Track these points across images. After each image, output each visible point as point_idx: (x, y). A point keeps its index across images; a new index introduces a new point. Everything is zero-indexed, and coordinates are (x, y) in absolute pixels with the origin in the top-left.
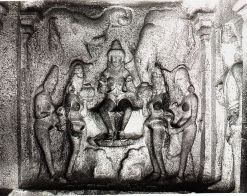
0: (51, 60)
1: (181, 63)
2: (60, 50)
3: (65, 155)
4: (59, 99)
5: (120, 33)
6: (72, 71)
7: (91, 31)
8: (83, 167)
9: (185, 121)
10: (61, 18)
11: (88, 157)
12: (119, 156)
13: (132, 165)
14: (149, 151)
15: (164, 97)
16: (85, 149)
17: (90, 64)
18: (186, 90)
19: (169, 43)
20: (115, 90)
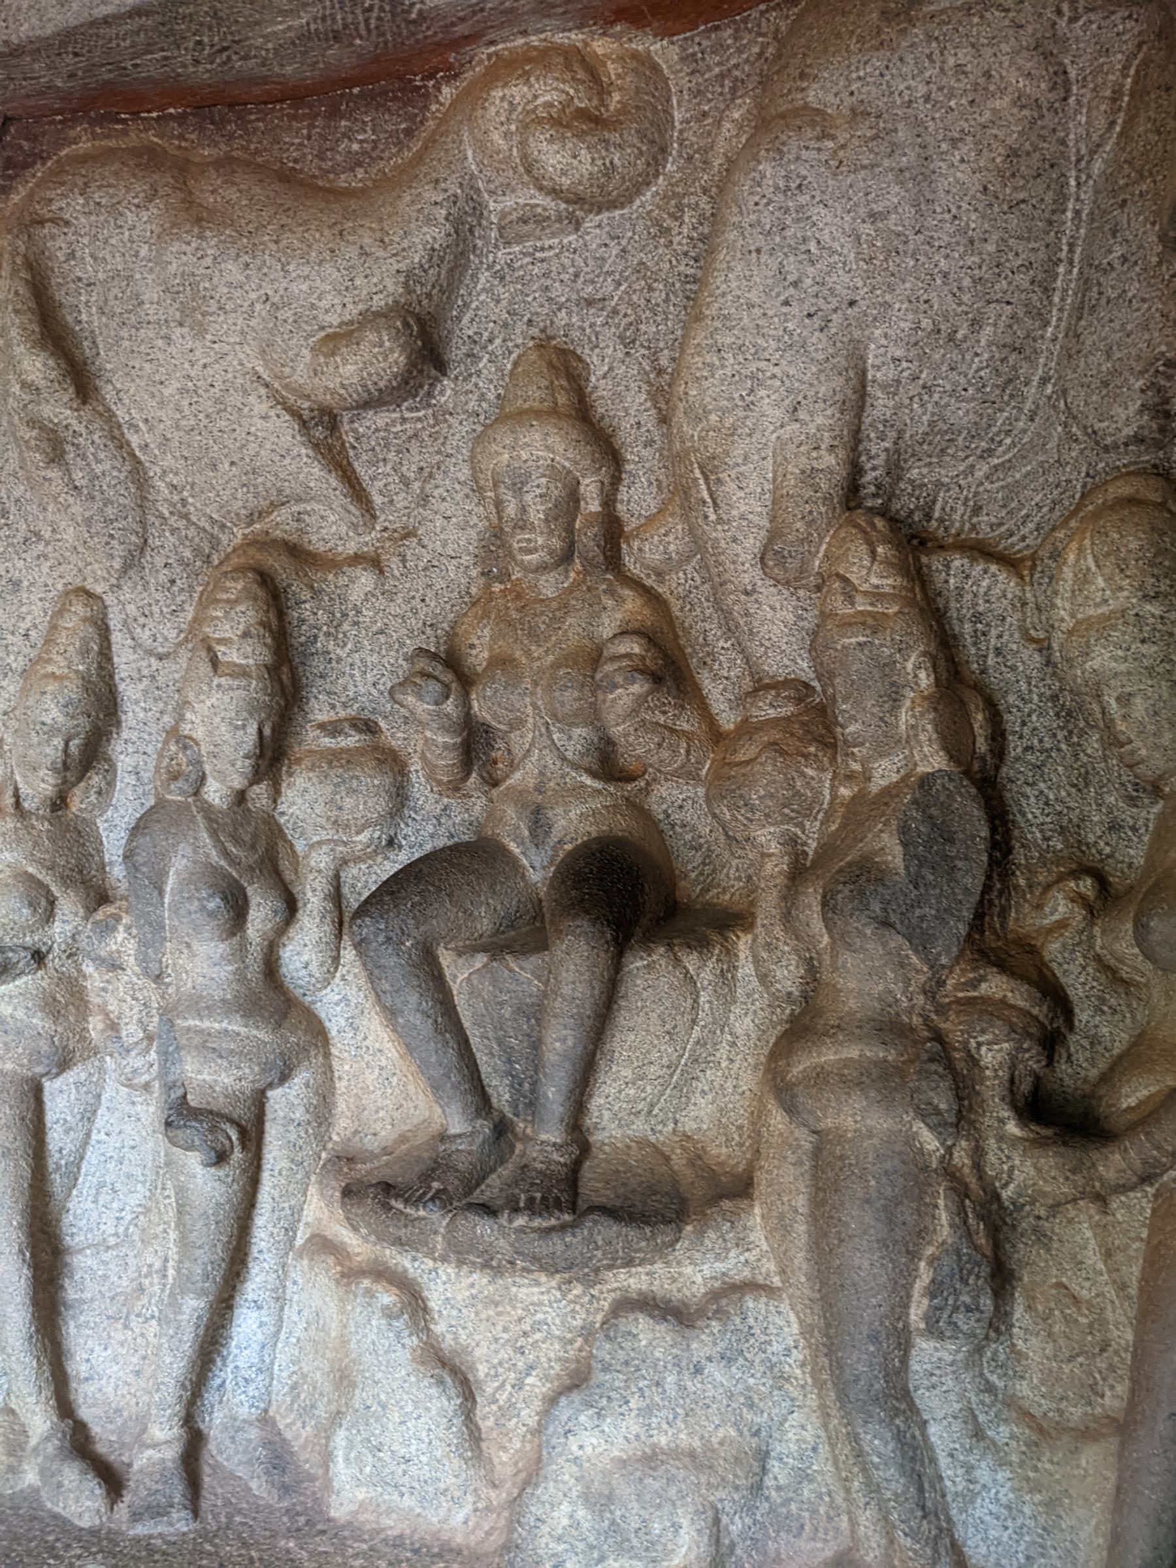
0: (50, 548)
5: (577, 275)
7: (304, 287)
8: (294, 1387)
10: (93, 218)
15: (934, 811)
17: (357, 559)
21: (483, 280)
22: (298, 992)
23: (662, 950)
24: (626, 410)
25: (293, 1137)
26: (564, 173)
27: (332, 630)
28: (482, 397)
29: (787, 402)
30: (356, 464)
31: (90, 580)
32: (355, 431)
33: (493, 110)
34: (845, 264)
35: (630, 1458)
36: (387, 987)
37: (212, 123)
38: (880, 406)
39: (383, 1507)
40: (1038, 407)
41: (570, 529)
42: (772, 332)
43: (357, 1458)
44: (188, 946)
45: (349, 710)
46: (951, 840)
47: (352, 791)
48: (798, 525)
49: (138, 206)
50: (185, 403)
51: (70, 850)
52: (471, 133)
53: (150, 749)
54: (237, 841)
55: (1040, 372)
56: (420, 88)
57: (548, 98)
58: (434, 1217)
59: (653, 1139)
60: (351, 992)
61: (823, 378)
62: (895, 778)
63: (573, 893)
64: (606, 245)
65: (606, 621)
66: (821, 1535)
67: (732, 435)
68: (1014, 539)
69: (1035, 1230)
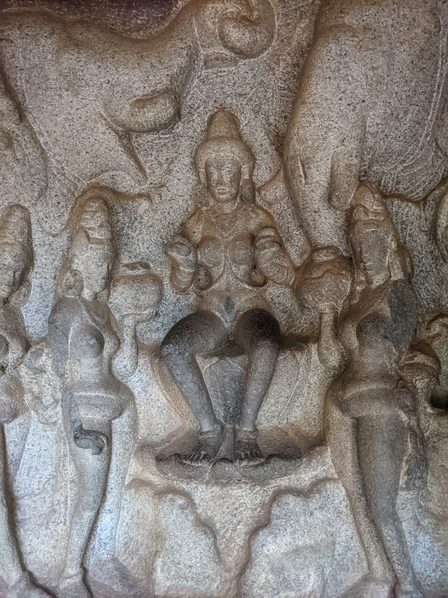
3: (62, 506)
7: (126, 78)
8: (125, 544)
10: (24, 40)
11: (138, 512)
12: (241, 513)
13: (286, 554)
14: (349, 495)
15: (398, 294)
16: (129, 487)
17: (140, 195)
19: (410, 93)
20: (223, 280)
21: (195, 82)
22: (120, 378)
23: (289, 352)
24: (256, 139)
25: (124, 439)
26: (238, 41)
27: (130, 225)
28: (195, 131)
29: (340, 138)
30: (138, 156)
31: (22, 201)
32: (138, 142)
33: (208, 12)
34: (362, 86)
35: (288, 552)
36: (179, 373)
38: (370, 141)
39: (179, 587)
40: (424, 145)
41: (238, 185)
42: (335, 110)
43: (167, 569)
44: (79, 360)
45: (137, 259)
46: (404, 305)
48: (345, 185)
49: (46, 37)
50: (67, 125)
51: (12, 321)
52: (197, 20)
53: (48, 276)
54: (98, 315)
55: (425, 132)
57: (232, 10)
58: (206, 466)
59: (279, 426)
61: (354, 129)
62: (382, 282)
63: (260, 331)
64: (247, 72)
66: (356, 570)
67: (317, 149)
68: (414, 194)
69: (434, 447)
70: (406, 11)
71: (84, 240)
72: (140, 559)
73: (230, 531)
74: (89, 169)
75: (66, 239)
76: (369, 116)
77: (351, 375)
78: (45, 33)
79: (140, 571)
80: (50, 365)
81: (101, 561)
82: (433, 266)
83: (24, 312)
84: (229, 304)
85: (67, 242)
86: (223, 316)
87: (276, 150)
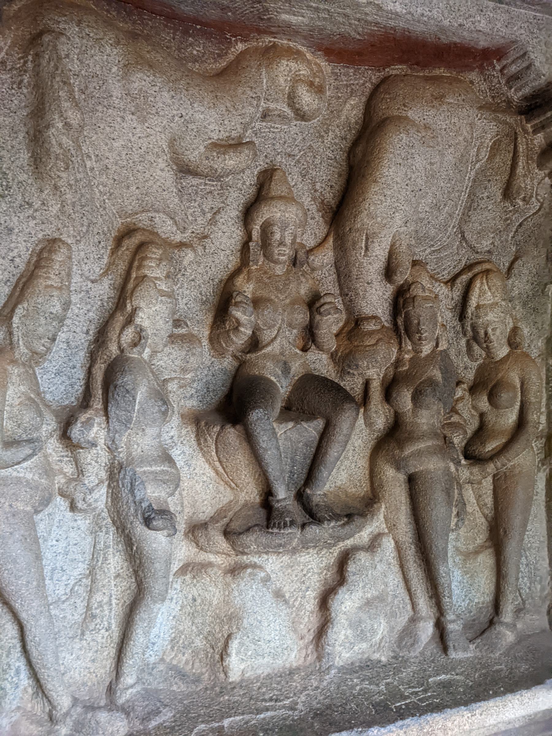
1: (479, 257)
2: (79, 176)
3: (106, 607)
4: (68, 382)
6: (122, 267)
7: (202, 117)
8: (172, 640)
9: (504, 441)
11: (194, 600)
12: (309, 578)
18: (504, 341)
28: (244, 183)
37: (125, 11)
39: (255, 667)
47: (194, 354)
49: (111, 45)
53: (78, 330)
56: (228, 39)
60: (187, 449)
65: (303, 287)
70: (456, 120)
71: (152, 293)
72: (195, 653)
73: (299, 599)
74: (131, 205)
75: (107, 287)
76: (421, 203)
77: (406, 435)
78: (110, 39)
79: (197, 664)
80: (103, 437)
81: (148, 665)
82: (455, 339)
83: (40, 373)
84: (286, 370)
85: (108, 290)
86: (279, 382)
87: (322, 217)
